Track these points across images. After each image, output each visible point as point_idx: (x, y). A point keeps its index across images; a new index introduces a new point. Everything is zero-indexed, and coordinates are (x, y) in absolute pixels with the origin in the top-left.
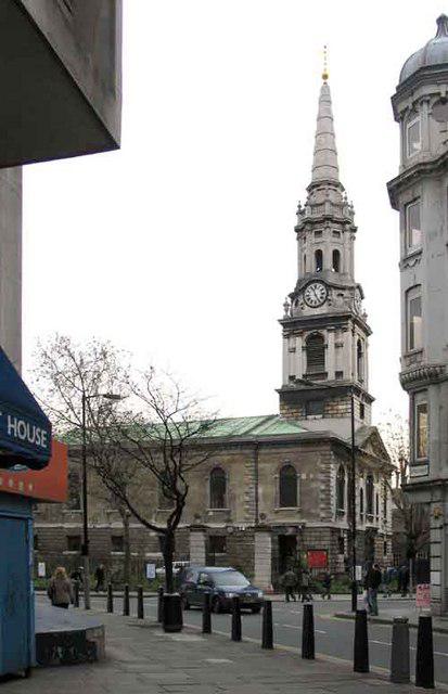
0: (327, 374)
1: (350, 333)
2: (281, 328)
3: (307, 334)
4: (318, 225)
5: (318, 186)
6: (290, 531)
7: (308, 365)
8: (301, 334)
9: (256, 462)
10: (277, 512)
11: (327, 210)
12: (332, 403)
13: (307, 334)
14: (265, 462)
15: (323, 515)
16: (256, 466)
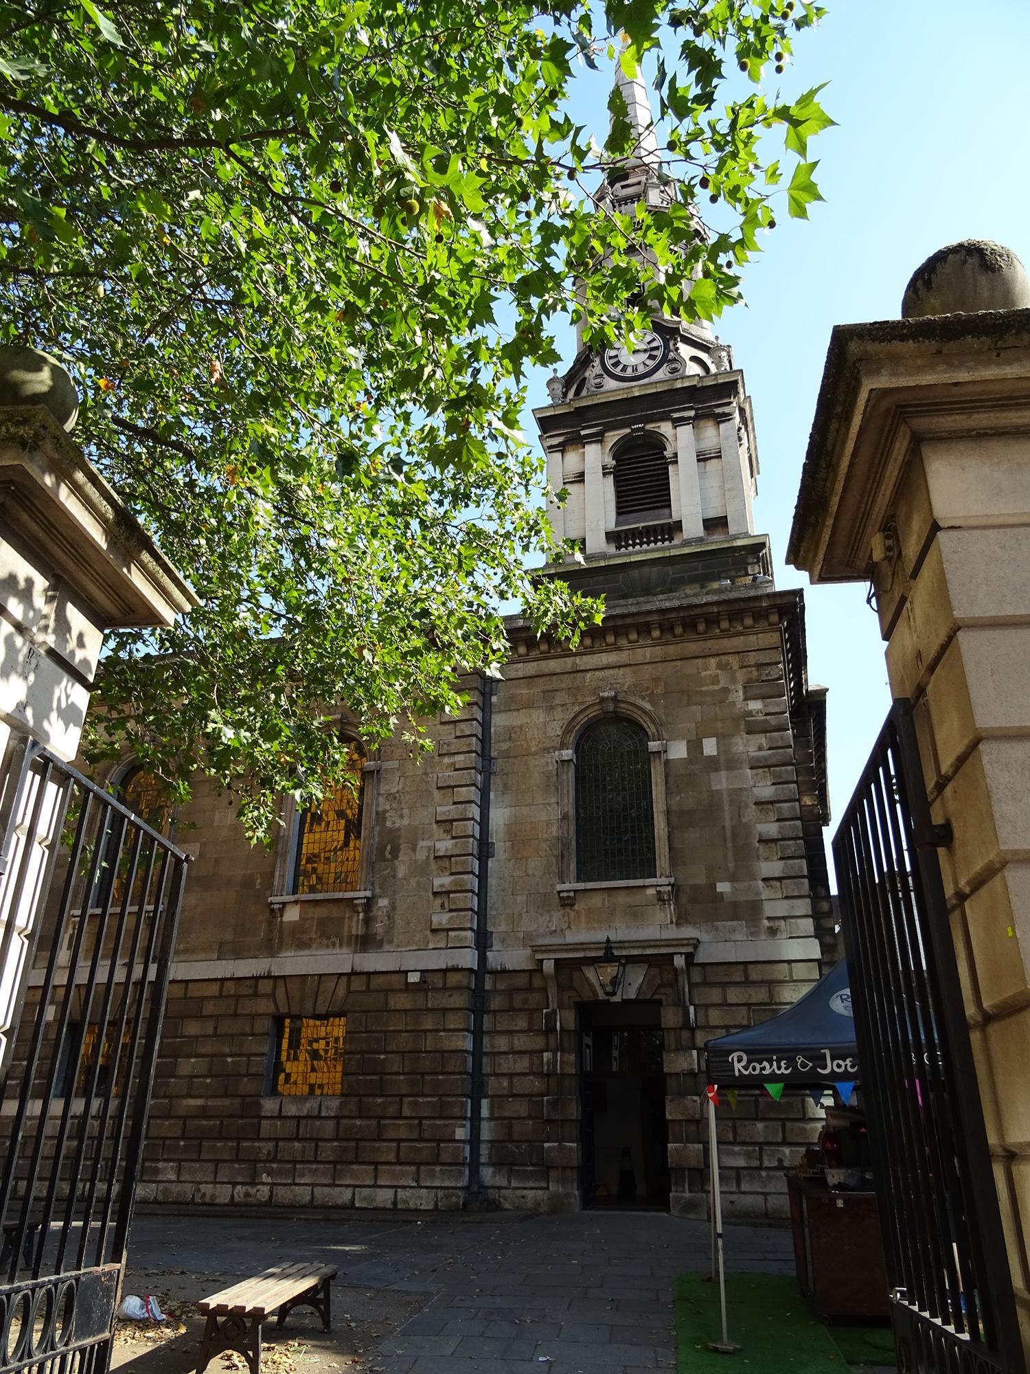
3: (613, 437)
6: (634, 983)
7: (618, 514)
8: (598, 438)
10: (567, 902)
13: (613, 437)
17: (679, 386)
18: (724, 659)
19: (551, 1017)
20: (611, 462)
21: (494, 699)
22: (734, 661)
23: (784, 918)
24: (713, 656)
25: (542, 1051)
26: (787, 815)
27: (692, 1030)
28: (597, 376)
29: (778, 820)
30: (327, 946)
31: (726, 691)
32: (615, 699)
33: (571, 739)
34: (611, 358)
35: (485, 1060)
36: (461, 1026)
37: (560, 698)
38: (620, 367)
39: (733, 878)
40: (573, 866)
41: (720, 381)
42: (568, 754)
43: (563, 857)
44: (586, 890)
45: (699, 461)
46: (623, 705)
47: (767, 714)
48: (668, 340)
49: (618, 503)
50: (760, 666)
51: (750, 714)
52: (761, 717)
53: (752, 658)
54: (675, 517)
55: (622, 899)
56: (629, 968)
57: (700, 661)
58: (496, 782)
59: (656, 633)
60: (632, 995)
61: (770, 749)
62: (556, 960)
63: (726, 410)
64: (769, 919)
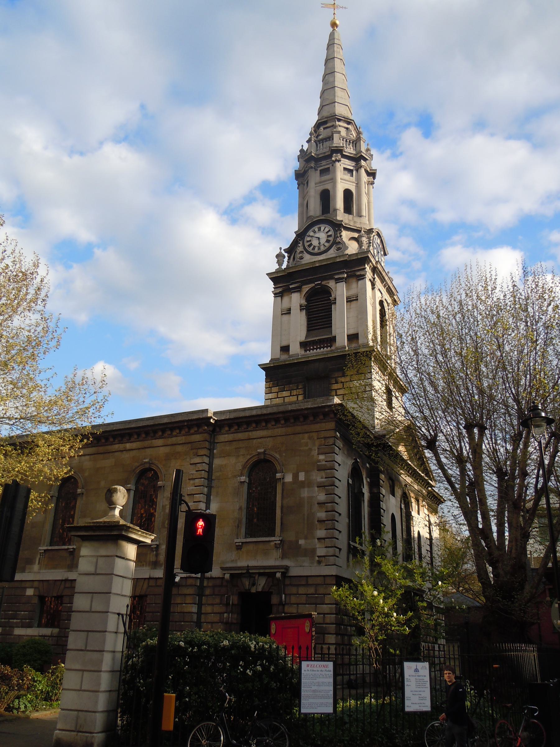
0: (334, 339)
1: (369, 285)
2: (271, 284)
3: (306, 288)
4: (324, 163)
5: (325, 123)
6: (261, 583)
7: (308, 331)
8: (298, 290)
9: (211, 457)
11: (337, 142)
12: (343, 379)
13: (306, 288)
14: (226, 455)
15: (321, 551)
16: (210, 465)
17: (338, 260)
18: (311, 434)
19: (228, 599)
20: (304, 302)
21: (215, 451)
22: (315, 435)
23: (324, 556)
24: (307, 433)
25: (224, 613)
26: (330, 509)
27: (284, 605)
28: (302, 252)
29: (326, 512)
30: (141, 566)
31: (310, 450)
32: (264, 453)
33: (246, 471)
34: (308, 241)
35: (203, 616)
36: (191, 602)
37: (242, 451)
38: (312, 247)
39: (306, 538)
40: (243, 530)
41: (359, 257)
42: (243, 478)
43: (238, 527)
44: (246, 542)
45: (347, 302)
46: (267, 456)
47: (326, 462)
48: (337, 231)
49: (308, 324)
50: (325, 438)
51: (319, 461)
52: (324, 463)
53: (323, 434)
54: (333, 334)
55: (261, 546)
56: (260, 578)
57: (301, 435)
58: (214, 491)
59: (283, 422)
60: (260, 589)
61: (326, 478)
62: (231, 574)
63: (362, 273)
64: (318, 556)
